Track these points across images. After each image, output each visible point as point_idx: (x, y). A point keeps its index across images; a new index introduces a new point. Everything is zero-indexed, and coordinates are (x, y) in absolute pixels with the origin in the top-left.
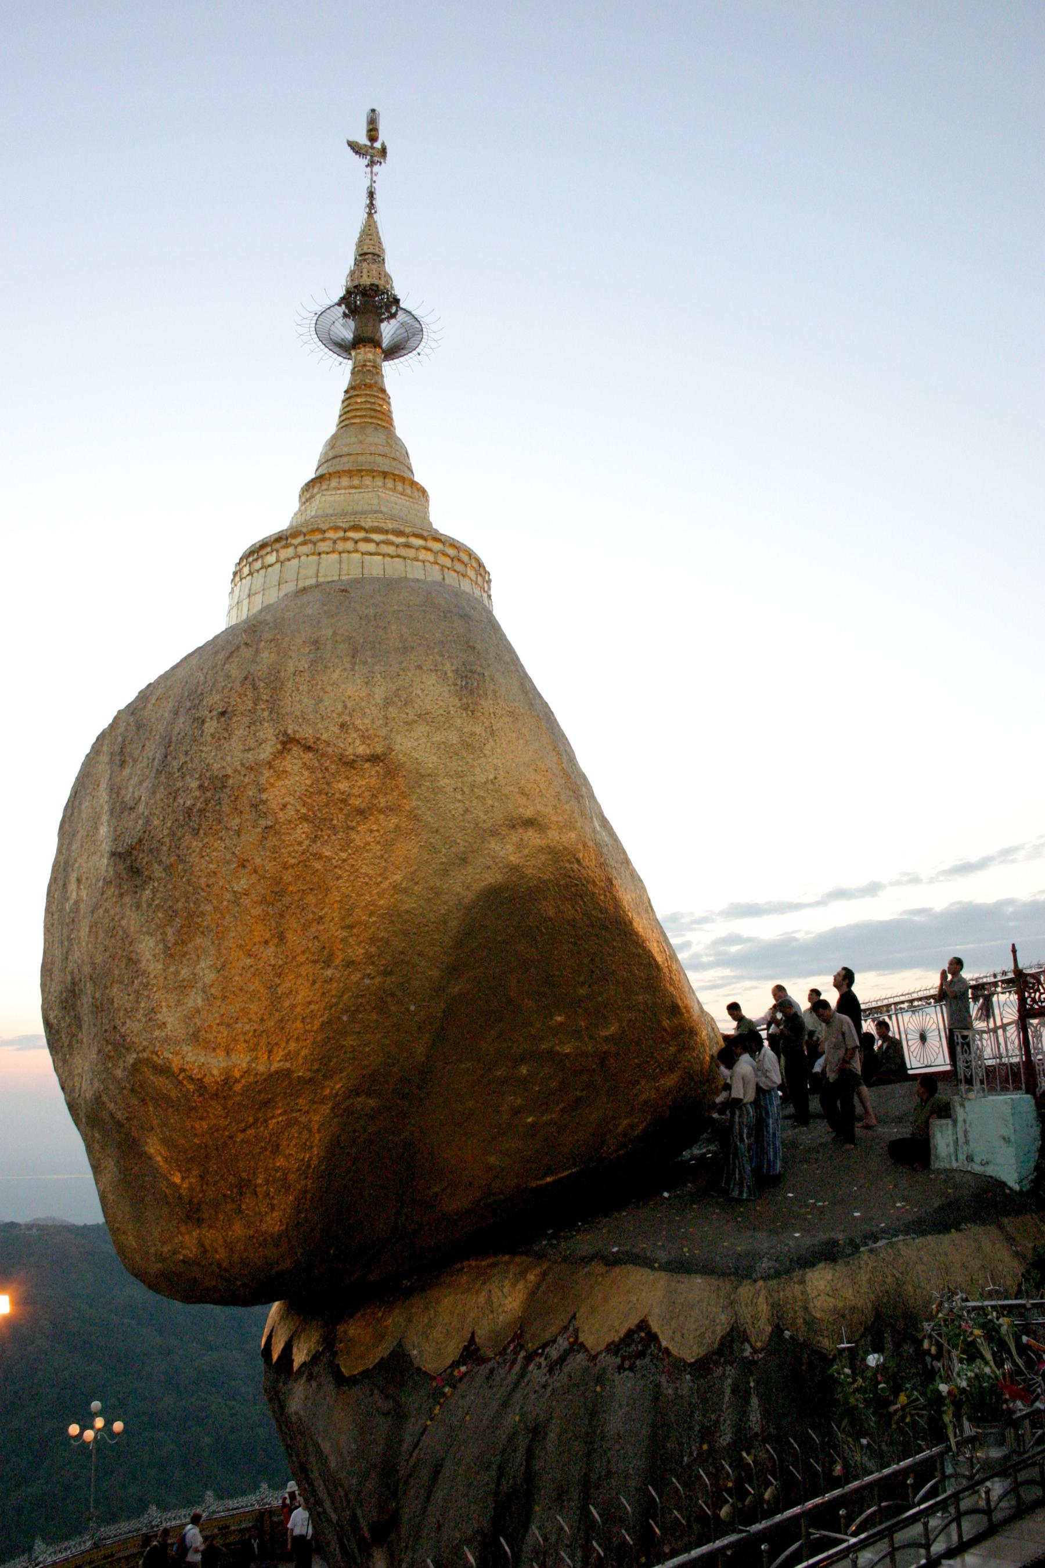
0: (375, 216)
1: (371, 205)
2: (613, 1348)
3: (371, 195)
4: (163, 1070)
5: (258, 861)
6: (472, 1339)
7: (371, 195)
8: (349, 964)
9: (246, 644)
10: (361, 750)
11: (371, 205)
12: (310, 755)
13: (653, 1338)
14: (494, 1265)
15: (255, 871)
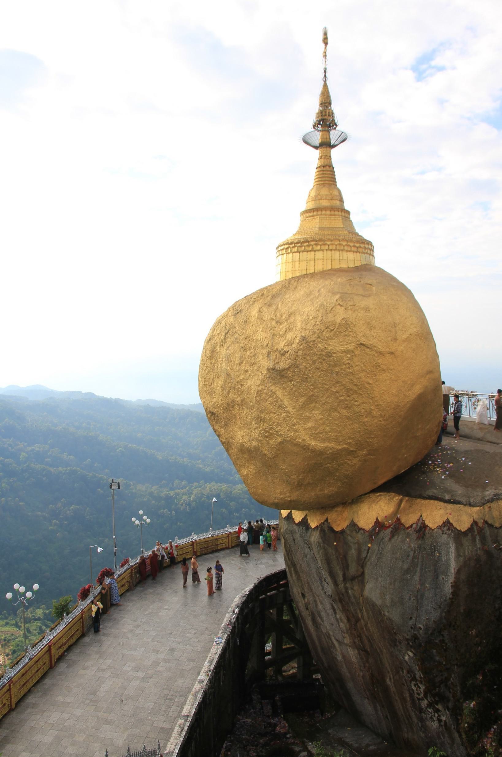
0: (327, 82)
1: (325, 76)
2: (440, 527)
3: (325, 72)
4: (297, 445)
5: (344, 383)
6: (377, 519)
7: (325, 72)
8: (373, 417)
9: (339, 305)
10: (387, 350)
11: (325, 76)
12: (368, 350)
13: (451, 524)
14: (381, 495)
15: (342, 385)
